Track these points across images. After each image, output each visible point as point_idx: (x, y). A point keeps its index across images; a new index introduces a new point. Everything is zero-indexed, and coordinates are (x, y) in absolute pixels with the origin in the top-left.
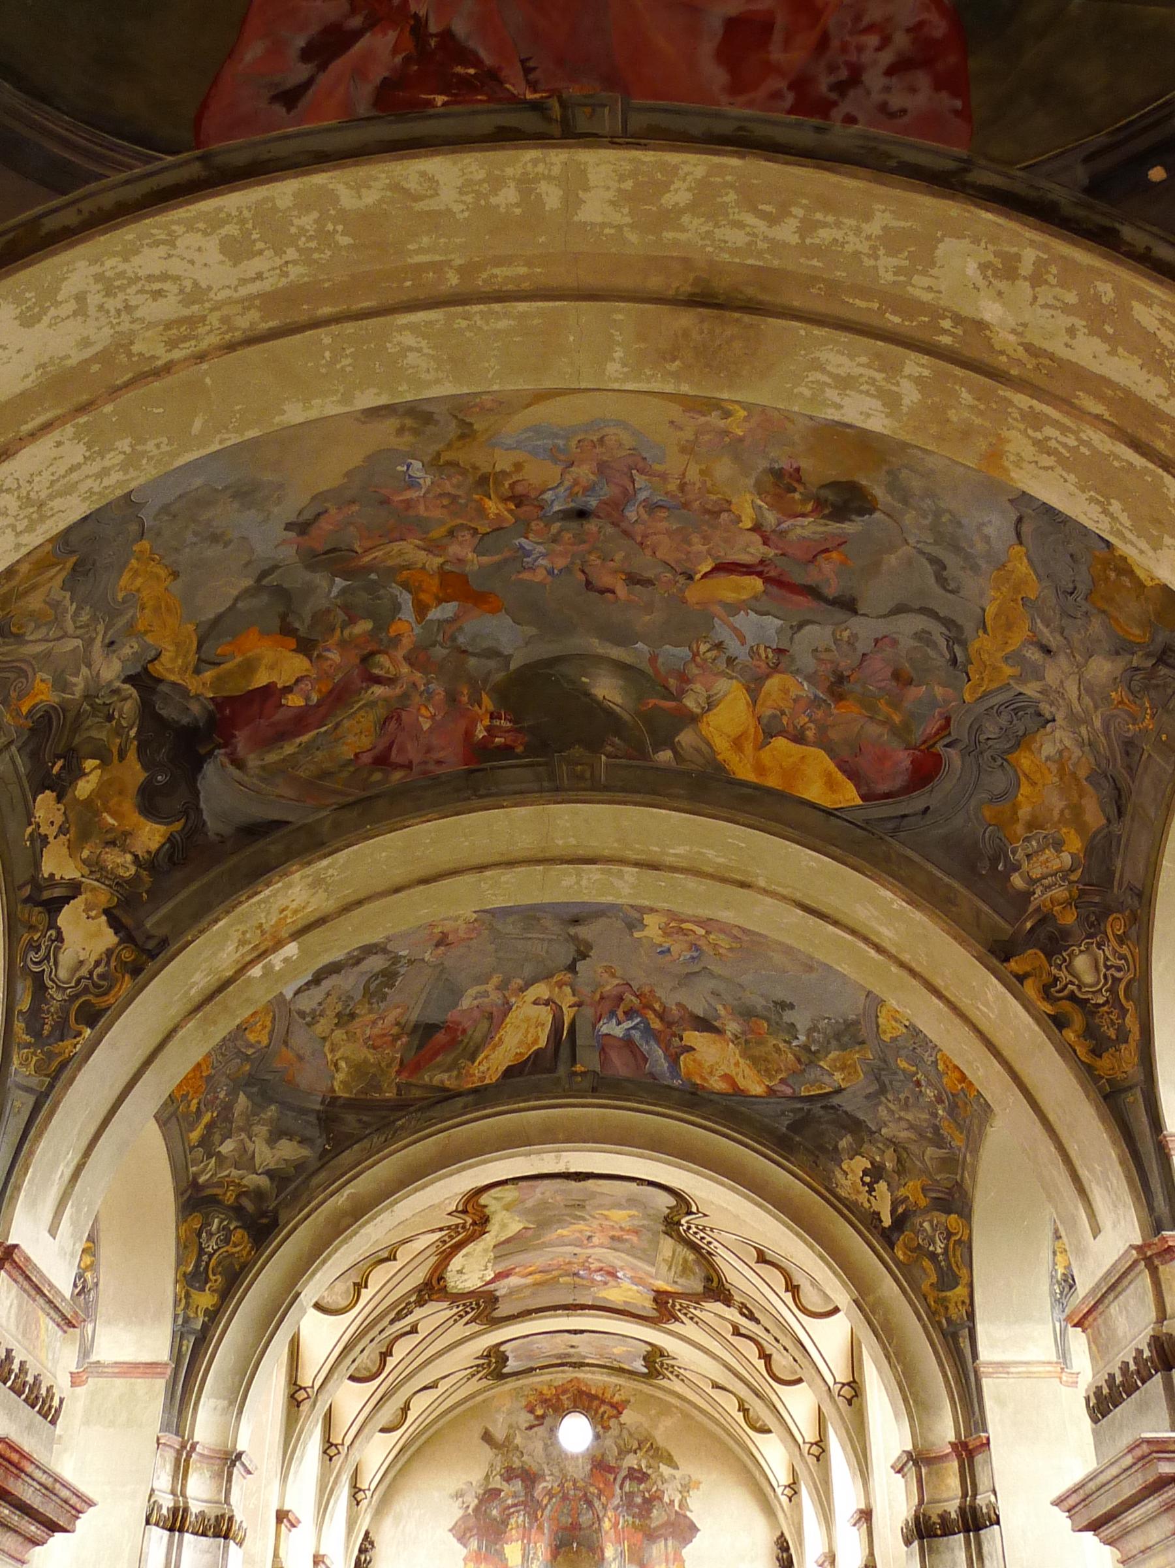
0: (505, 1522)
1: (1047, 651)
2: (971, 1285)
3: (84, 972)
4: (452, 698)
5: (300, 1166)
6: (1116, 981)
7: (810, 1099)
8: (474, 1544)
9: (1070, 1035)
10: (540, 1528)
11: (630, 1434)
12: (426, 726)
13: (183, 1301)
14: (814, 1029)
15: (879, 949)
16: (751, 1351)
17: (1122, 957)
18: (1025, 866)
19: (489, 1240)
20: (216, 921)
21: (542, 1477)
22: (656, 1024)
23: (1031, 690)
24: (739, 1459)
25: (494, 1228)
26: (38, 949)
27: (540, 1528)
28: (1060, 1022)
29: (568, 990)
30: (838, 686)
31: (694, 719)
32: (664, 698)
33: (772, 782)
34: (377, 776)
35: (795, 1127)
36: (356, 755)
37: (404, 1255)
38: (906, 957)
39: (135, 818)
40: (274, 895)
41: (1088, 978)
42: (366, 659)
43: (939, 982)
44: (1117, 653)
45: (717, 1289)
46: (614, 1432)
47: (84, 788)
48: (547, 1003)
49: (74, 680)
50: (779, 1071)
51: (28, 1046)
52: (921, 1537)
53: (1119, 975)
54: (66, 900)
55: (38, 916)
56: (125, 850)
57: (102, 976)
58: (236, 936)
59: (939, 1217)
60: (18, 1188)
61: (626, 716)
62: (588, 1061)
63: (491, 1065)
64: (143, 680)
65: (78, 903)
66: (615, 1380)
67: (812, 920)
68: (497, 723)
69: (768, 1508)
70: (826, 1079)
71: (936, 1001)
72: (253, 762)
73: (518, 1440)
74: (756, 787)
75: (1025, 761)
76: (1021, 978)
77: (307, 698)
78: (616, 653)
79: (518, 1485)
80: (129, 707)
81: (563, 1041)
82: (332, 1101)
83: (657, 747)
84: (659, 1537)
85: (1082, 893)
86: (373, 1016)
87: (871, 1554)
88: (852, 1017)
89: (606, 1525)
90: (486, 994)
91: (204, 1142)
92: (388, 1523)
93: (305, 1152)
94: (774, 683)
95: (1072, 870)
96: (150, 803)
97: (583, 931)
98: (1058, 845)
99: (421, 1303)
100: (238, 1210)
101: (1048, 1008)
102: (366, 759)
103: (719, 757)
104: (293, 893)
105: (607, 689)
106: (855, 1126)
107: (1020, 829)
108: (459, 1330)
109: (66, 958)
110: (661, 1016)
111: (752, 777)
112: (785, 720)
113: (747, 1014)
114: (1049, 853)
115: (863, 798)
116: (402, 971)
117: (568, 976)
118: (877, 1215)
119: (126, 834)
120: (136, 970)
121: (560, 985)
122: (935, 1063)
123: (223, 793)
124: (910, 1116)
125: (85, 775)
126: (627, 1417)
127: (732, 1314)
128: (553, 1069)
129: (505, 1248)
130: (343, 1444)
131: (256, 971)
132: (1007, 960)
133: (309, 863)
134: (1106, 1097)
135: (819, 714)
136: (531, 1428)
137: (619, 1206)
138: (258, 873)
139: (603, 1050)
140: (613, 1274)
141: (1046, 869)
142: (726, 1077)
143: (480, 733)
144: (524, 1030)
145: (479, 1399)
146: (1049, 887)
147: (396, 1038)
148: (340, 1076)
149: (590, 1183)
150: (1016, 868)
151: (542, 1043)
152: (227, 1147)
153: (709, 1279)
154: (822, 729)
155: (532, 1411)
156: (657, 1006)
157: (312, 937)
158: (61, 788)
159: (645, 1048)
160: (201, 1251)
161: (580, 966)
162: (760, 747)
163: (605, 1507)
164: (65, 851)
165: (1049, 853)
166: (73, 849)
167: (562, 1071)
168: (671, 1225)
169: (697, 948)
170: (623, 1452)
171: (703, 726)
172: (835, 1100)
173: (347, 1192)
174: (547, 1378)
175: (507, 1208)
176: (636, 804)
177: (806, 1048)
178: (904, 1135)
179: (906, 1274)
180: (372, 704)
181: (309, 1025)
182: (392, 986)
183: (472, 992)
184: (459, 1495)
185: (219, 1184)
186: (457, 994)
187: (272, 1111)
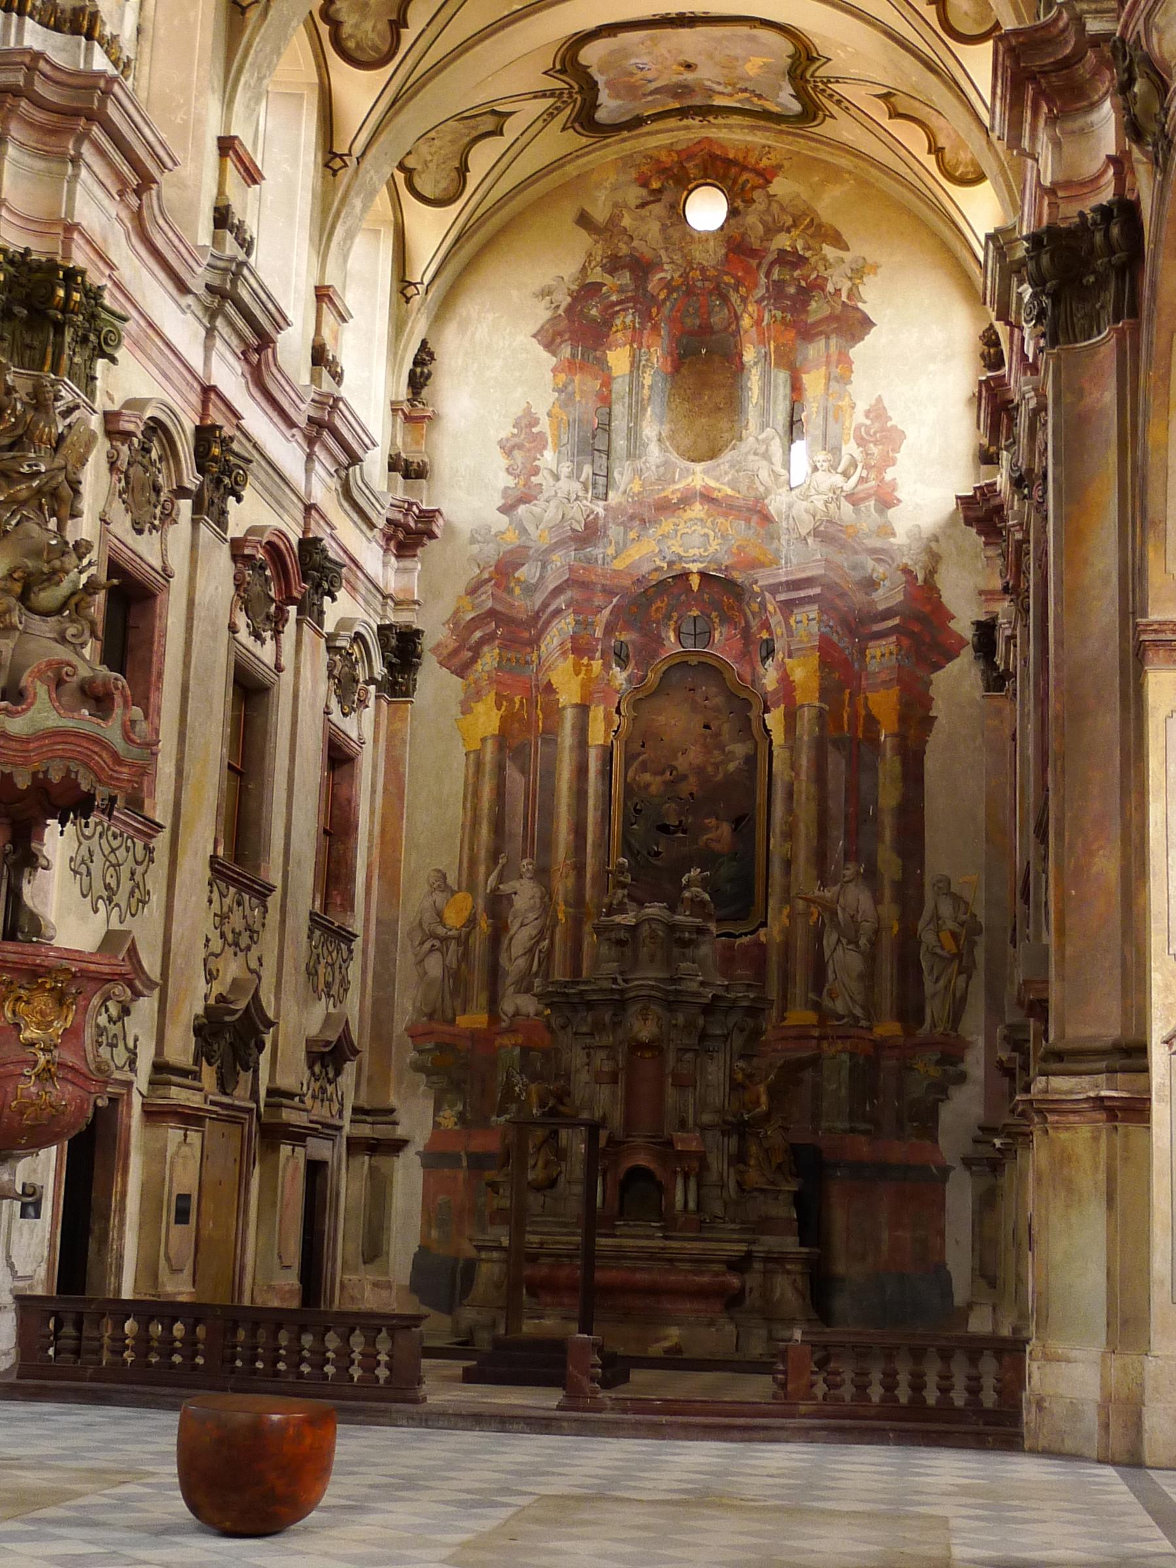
0: (608, 323)
8: (566, 351)
10: (655, 328)
11: (783, 209)
24: (935, 235)
27: (655, 328)
46: (760, 205)
66: (758, 139)
73: (626, 222)
79: (626, 278)
84: (821, 333)
89: (746, 322)
126: (780, 186)
130: (350, 154)
136: (643, 205)
145: (571, 170)
155: (645, 184)
163: (744, 300)
170: (771, 230)
174: (664, 139)
184: (546, 292)
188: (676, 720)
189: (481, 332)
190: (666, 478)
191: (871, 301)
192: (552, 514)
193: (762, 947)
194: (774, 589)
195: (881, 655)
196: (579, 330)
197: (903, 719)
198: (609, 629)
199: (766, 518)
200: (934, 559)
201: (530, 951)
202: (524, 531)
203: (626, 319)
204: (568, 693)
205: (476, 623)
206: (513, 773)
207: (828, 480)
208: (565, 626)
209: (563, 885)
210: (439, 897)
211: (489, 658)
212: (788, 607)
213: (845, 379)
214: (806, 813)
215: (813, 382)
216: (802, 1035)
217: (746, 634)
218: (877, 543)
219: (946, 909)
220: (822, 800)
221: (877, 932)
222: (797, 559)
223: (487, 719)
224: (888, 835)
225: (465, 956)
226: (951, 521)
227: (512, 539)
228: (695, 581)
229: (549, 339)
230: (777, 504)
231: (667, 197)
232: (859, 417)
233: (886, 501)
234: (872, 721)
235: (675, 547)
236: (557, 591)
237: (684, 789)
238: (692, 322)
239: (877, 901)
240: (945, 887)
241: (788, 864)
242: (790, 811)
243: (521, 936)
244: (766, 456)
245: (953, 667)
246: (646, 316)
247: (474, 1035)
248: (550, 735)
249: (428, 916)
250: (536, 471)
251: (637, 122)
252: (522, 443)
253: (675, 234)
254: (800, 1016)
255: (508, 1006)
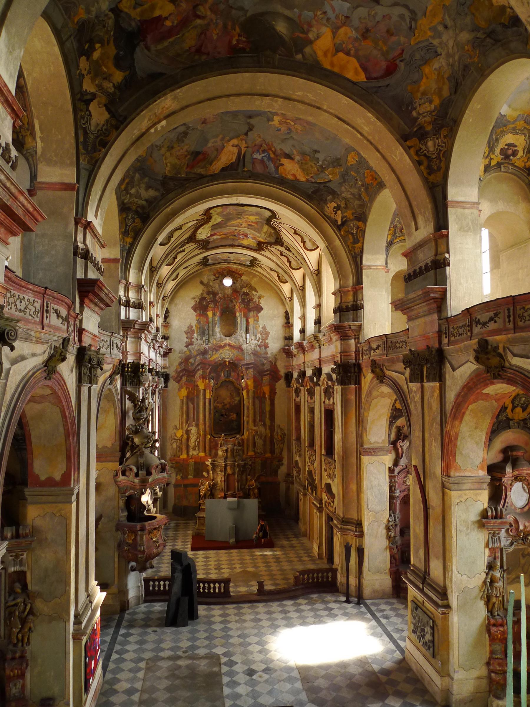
1: (446, 27)
2: (363, 243)
3: (99, 128)
4: (225, 26)
5: (155, 198)
6: (440, 150)
7: (320, 183)
8: (199, 312)
9: (422, 168)
10: (218, 308)
12: (215, 37)
13: (122, 240)
14: (324, 160)
15: (361, 134)
16: (285, 260)
17: (444, 143)
18: (418, 108)
19: (211, 224)
20: (142, 111)
21: (218, 294)
22: (272, 156)
23: (435, 42)
25: (213, 220)
26: (84, 119)
28: (420, 163)
29: (244, 142)
30: (365, 33)
31: (311, 42)
32: (302, 33)
33: (336, 70)
34: (197, 57)
35: (314, 192)
36: (190, 48)
37: (184, 229)
38: (370, 138)
39: (113, 69)
40: (161, 102)
41: (431, 149)
42: (195, 7)
43: (380, 147)
44: (473, 31)
45: (279, 241)
47: (96, 55)
48: (236, 146)
49: (92, 9)
50: (311, 173)
51: (84, 154)
52: (340, 312)
53: (442, 149)
54: (91, 100)
55: (82, 106)
56: (110, 82)
57: (106, 130)
58: (148, 117)
59: (356, 222)
60: (88, 203)
61: (287, 39)
62: (249, 167)
63: (217, 166)
64: (116, 11)
65: (95, 102)
66: (239, 267)
67: (340, 122)
68: (240, 38)
69: (283, 304)
70: (326, 177)
71: (377, 153)
72: (153, 48)
73: (211, 284)
74: (330, 72)
75: (427, 69)
76: (410, 148)
77: (173, 23)
78: (287, 12)
79: (211, 296)
80: (111, 22)
81: (241, 159)
82: (165, 177)
83: (297, 53)
85: (435, 119)
86: (179, 148)
87: (320, 316)
88: (339, 157)
89: (237, 307)
90: (216, 142)
91: (126, 189)
92: (173, 305)
93: (157, 194)
94: (342, 30)
95: (434, 111)
96: (118, 63)
97: (252, 121)
98: (431, 102)
99: (188, 243)
100: (136, 212)
101: (416, 158)
102: (193, 50)
103: (319, 59)
104: (167, 102)
105: (281, 27)
106: (333, 193)
107: (419, 95)
108: (197, 252)
109: (93, 122)
110: (274, 153)
111: (329, 67)
112: (344, 46)
113: (303, 154)
114: (427, 104)
115: (367, 79)
116: (190, 132)
117: (245, 137)
118: (336, 221)
119: (110, 75)
120: (117, 128)
121: (242, 140)
122: (364, 174)
123: (144, 60)
124: (352, 190)
125: (96, 50)
126: (243, 278)
127: (283, 249)
128: (237, 170)
129: (214, 227)
131: (152, 130)
132: (405, 141)
133: (173, 90)
134: (430, 188)
135: (357, 44)
137: (253, 215)
138: (155, 94)
139: (253, 163)
140: (246, 236)
141: (425, 110)
142: (294, 175)
143: (234, 42)
144: (228, 155)
146: (424, 117)
147: (186, 156)
148: (168, 169)
149: (245, 208)
150: (415, 109)
151: (234, 160)
152: (133, 191)
153: (277, 238)
154: (357, 50)
156: (273, 149)
157: (170, 119)
158: (88, 54)
159: (267, 163)
160: (126, 225)
161: (249, 133)
162: (335, 55)
164: (90, 81)
165: (427, 104)
166: (93, 80)
167: (240, 170)
168: (268, 221)
169: (290, 129)
170: (242, 287)
171: (314, 45)
172: (328, 184)
173: (171, 207)
175: (218, 214)
176: (288, 75)
177: (321, 166)
178: (349, 196)
179: (344, 239)
180: (196, 27)
181: (159, 150)
182: (186, 137)
183: (212, 141)
184: (194, 298)
185: (131, 203)
186: (207, 141)
187: (146, 179)
188: (224, 393)
189: (180, 307)
190: (220, 340)
191: (263, 304)
192: (196, 348)
193: (243, 440)
194: (244, 365)
195: (266, 379)
196: (201, 307)
197: (270, 392)
198: (210, 373)
199: (242, 350)
200: (276, 359)
201: (195, 442)
202: (190, 351)
203: (211, 305)
204: (201, 387)
205: (180, 371)
206: (190, 404)
207: (254, 342)
208: (200, 372)
209: (201, 427)
210: (175, 431)
211: (184, 379)
212: (247, 369)
213: (257, 321)
214: (251, 412)
215: (251, 321)
216: (251, 457)
217: (238, 374)
218: (265, 356)
219: (279, 431)
220: (254, 409)
221: (266, 436)
222: (248, 359)
223: (184, 392)
224: (268, 416)
225: (181, 443)
226: (280, 350)
227: (188, 353)
228: (227, 363)
229: (195, 309)
230: (244, 347)
231: (220, 279)
232: (261, 329)
233: (266, 347)
234: (264, 393)
235: (223, 356)
236: (198, 365)
237: (226, 407)
238: (225, 306)
239: (266, 430)
240: (279, 427)
241: (248, 423)
242: (248, 411)
243: (193, 439)
244: (242, 336)
245: (280, 382)
246: (216, 305)
247: (184, 459)
248: (198, 396)
249: (173, 435)
250: (193, 338)
251: (215, 264)
252: (189, 332)
253: (222, 287)
254: (251, 453)
255: (191, 453)
